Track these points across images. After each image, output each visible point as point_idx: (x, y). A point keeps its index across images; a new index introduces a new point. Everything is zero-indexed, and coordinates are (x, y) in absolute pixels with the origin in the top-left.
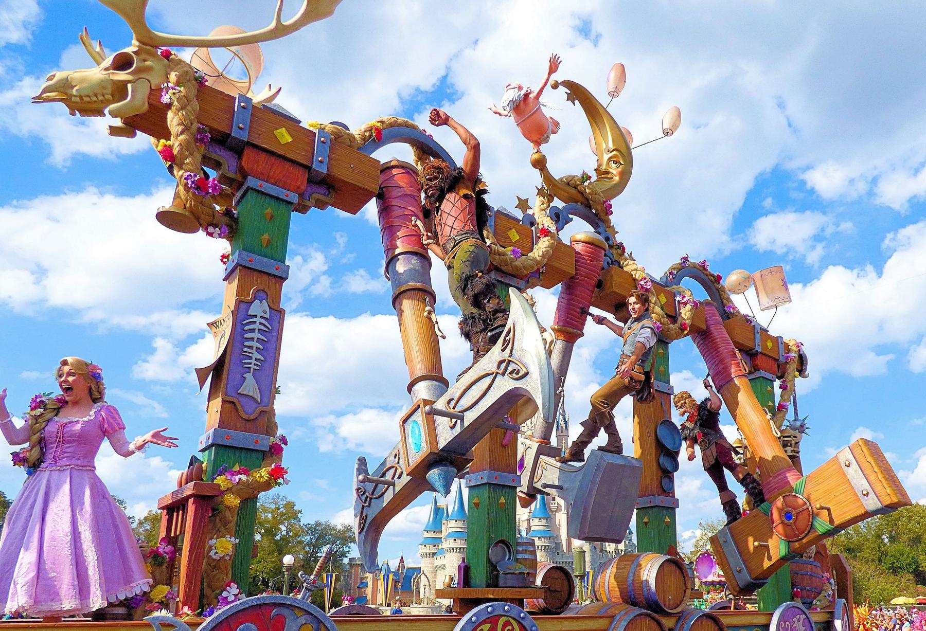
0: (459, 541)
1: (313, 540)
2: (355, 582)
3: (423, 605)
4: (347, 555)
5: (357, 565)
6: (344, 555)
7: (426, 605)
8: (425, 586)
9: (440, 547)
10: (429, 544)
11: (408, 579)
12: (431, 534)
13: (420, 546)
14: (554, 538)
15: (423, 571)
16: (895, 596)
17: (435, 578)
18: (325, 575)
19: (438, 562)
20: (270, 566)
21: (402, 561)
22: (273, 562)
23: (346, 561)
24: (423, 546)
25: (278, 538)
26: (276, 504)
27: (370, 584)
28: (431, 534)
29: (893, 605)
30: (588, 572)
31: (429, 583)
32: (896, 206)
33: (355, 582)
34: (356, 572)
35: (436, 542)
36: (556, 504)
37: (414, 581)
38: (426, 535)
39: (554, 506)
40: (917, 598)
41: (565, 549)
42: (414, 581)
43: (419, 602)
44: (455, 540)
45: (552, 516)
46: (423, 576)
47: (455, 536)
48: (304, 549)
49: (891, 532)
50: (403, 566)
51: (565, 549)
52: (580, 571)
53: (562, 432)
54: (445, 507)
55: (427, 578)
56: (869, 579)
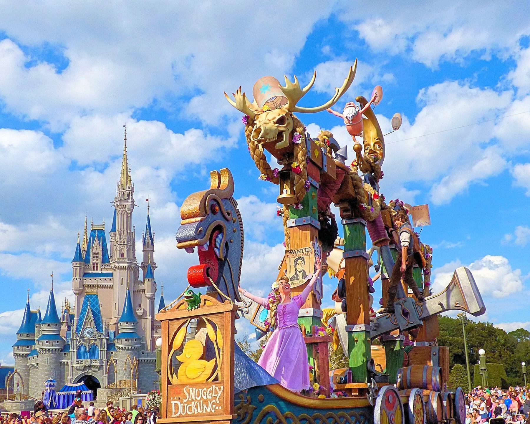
3: (16, 401)
8: (18, 384)
9: (33, 348)
14: (140, 339)
15: (16, 370)
17: (28, 375)
19: (31, 361)
28: (24, 337)
31: (22, 380)
32: (428, 64)
35: (29, 343)
36: (142, 309)
37: (8, 379)
39: (139, 312)
41: (149, 348)
42: (8, 379)
43: (12, 398)
44: (47, 342)
45: (138, 320)
47: (47, 338)
51: (149, 348)
53: (148, 247)
55: (20, 376)
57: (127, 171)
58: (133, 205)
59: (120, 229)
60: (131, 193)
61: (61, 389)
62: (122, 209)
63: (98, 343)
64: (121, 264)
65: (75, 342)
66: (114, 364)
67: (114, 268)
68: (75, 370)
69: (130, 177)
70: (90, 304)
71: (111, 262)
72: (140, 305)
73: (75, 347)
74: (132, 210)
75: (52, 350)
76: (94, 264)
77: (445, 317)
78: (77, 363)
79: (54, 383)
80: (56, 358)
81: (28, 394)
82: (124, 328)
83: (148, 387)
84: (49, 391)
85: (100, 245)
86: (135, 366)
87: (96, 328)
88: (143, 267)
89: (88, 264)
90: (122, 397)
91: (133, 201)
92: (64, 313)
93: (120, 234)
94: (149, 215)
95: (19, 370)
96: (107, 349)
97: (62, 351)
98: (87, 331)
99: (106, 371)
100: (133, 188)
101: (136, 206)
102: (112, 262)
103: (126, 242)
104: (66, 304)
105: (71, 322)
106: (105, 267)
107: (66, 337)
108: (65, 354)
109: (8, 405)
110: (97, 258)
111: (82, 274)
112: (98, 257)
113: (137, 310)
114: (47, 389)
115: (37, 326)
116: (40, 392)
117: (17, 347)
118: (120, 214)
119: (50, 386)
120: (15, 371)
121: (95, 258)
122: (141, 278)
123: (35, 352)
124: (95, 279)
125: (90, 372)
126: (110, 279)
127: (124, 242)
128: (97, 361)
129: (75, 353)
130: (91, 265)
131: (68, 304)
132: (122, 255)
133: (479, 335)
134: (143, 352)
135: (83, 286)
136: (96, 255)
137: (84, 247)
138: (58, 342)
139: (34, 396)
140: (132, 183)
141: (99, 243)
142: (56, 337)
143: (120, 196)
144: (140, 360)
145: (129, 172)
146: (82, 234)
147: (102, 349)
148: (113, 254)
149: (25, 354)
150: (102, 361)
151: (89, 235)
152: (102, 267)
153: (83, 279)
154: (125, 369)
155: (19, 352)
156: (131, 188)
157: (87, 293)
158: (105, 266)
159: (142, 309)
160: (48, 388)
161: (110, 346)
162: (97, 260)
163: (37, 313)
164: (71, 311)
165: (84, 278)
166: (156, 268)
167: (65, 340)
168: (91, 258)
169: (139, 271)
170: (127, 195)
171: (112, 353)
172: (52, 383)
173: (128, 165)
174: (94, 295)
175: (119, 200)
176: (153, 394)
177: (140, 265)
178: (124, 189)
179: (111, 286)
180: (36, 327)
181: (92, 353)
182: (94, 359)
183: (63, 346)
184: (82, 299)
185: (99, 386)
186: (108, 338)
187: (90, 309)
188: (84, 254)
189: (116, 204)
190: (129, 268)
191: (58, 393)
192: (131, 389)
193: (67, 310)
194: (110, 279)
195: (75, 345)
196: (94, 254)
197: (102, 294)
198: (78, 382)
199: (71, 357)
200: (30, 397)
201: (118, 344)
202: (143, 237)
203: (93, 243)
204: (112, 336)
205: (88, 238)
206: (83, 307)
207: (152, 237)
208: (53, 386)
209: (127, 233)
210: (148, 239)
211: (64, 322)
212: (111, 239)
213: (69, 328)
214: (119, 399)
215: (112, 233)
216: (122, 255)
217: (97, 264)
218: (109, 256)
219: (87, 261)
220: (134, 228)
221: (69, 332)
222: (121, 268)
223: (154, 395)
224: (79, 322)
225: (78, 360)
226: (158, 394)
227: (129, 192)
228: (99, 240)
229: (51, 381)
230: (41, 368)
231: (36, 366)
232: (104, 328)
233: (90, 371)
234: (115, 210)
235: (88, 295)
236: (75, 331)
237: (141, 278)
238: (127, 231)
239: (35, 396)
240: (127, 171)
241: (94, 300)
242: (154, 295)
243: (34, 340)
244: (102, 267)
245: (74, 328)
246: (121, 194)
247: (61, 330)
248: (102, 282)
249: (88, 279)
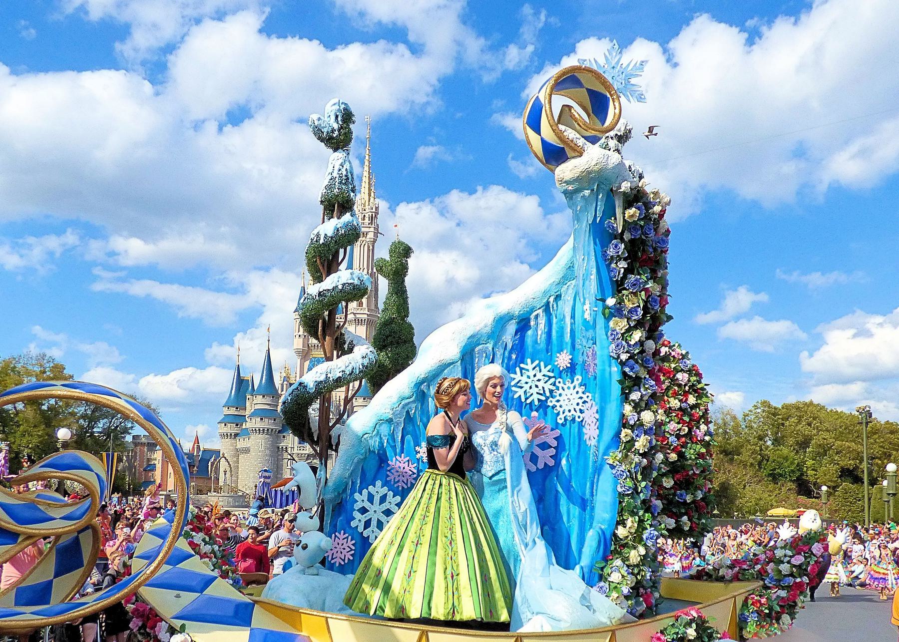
0: (266, 420)
1: (89, 412)
2: (142, 461)
3: (223, 494)
4: (130, 431)
5: (143, 444)
6: (126, 431)
7: (226, 494)
8: (225, 472)
9: (244, 427)
10: (229, 423)
11: (204, 462)
12: (232, 411)
13: (219, 425)
15: (223, 454)
16: (772, 507)
17: (238, 462)
18: (104, 454)
19: (241, 443)
20: (35, 441)
21: (197, 440)
22: (40, 436)
23: (129, 438)
24: (224, 425)
25: (45, 407)
26: (41, 366)
27: (159, 466)
28: (232, 411)
29: (770, 516)
31: (231, 468)
33: (142, 461)
34: (142, 452)
35: (238, 420)
37: (212, 466)
38: (226, 411)
40: (798, 510)
43: (218, 490)
44: (262, 419)
47: (261, 414)
48: (78, 422)
49: (777, 433)
50: (198, 447)
54: (250, 379)
55: (228, 462)
56: (745, 486)
58: (377, 233)
60: (374, 216)
64: (358, 316)
74: (374, 241)
75: (268, 430)
80: (272, 441)
91: (376, 229)
97: (279, 432)
100: (377, 208)
108: (284, 437)
109: (213, 499)
115: (249, 397)
118: (359, 245)
119: (265, 477)
120: (221, 456)
123: (247, 433)
157: (313, 356)
164: (291, 379)
172: (267, 474)
178: (365, 210)
184: (307, 363)
208: (269, 477)
211: (282, 393)
225: (300, 445)
227: (372, 215)
229: (265, 471)
230: (254, 454)
231: (247, 451)
238: (368, 270)
246: (360, 217)
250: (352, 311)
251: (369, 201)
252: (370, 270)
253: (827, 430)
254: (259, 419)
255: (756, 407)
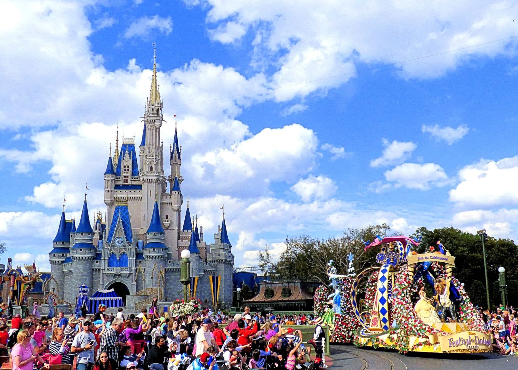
15: (53, 276)
17: (63, 281)
19: (66, 268)
28: (60, 245)
30: (194, 278)
36: (169, 221)
44: (81, 250)
45: (166, 232)
46: (52, 280)
52: (186, 277)
53: (175, 161)
54: (72, 222)
55: (56, 282)
57: (156, 87)
59: (149, 143)
60: (159, 109)
61: (93, 295)
62: (151, 124)
63: (127, 252)
65: (106, 250)
66: (143, 272)
67: (144, 181)
68: (106, 277)
69: (159, 93)
70: (121, 215)
71: (140, 175)
72: (167, 217)
73: (107, 256)
76: (125, 177)
77: (465, 233)
78: (108, 270)
79: (87, 289)
81: (63, 299)
82: (152, 238)
83: (174, 296)
84: (82, 297)
85: (130, 159)
86: (162, 275)
87: (126, 238)
88: (170, 181)
89: (119, 177)
90: (149, 304)
92: (97, 223)
93: (149, 148)
94: (176, 131)
95: (55, 276)
96: (136, 258)
97: (94, 259)
98: (116, 241)
99: (135, 279)
101: (164, 121)
102: (142, 175)
103: (154, 156)
104: (99, 214)
105: (103, 231)
106: (135, 180)
107: (98, 246)
110: (128, 171)
111: (113, 187)
112: (128, 170)
113: (164, 221)
114: (80, 295)
116: (74, 297)
117: (53, 255)
120: (51, 278)
121: (125, 172)
122: (168, 191)
123: (69, 259)
124: (125, 191)
125: (120, 280)
126: (139, 191)
127: (153, 156)
128: (126, 270)
129: (107, 262)
130: (122, 178)
131: (100, 215)
132: (151, 168)
133: (499, 252)
134: (169, 261)
135: (114, 197)
136: (126, 168)
137: (115, 161)
138: (90, 250)
139: (68, 301)
140: (161, 99)
141: (130, 156)
142: (89, 246)
143: (150, 112)
144: (167, 269)
145: (158, 89)
146: (114, 146)
147: (131, 258)
148: (142, 167)
149: (60, 261)
150: (131, 269)
151: (120, 149)
152: (132, 180)
153: (114, 191)
154: (152, 278)
155: (55, 259)
156: (160, 104)
158: (135, 178)
159: (169, 221)
160: (81, 293)
161: (139, 256)
162: (127, 173)
163: (71, 223)
164: (102, 221)
165: (116, 190)
166: (182, 181)
167: (97, 248)
168: (121, 171)
169: (166, 184)
170: (156, 110)
171: (140, 262)
172: (83, 289)
173: (157, 82)
174: (124, 206)
175: (148, 116)
176: (178, 303)
177: (168, 178)
178: (153, 105)
179: (140, 198)
180: (70, 236)
181: (122, 261)
182: (123, 268)
183: (95, 254)
185: (129, 294)
186: (137, 247)
187: (120, 219)
188: (115, 168)
189: (146, 119)
190: (157, 181)
191: (90, 299)
192: (158, 296)
193: (99, 221)
194: (139, 191)
195: (106, 253)
196: (125, 167)
197: (132, 206)
198: (109, 289)
199: (103, 265)
200: (65, 302)
201: (147, 253)
202: (171, 151)
203: (124, 156)
204: (141, 245)
205: (119, 152)
206: (114, 217)
207: (179, 151)
208: (86, 292)
209: (156, 147)
210: (175, 153)
211: (96, 231)
212: (141, 152)
213: (101, 237)
214: (146, 306)
215: (142, 147)
216: (151, 168)
217: (128, 177)
218: (139, 169)
219: (118, 174)
220: (162, 142)
221: (100, 241)
222: (149, 180)
223: (179, 304)
224: (110, 232)
225: (109, 268)
226: (182, 303)
228: (130, 154)
229: (84, 287)
230: (75, 275)
231: (70, 273)
232: (134, 237)
233: (120, 278)
234: (145, 126)
235: (119, 206)
236: (106, 240)
237: (168, 191)
239: (70, 301)
240: (156, 87)
241: (124, 211)
242: (180, 207)
243: (69, 248)
244: (132, 180)
245: (106, 237)
246: (150, 110)
247: (94, 239)
248: (132, 193)
249: (118, 191)
250: (146, 173)
251: (156, 99)
252: (157, 146)
253: (463, 246)
254: (79, 250)
255: (418, 232)
